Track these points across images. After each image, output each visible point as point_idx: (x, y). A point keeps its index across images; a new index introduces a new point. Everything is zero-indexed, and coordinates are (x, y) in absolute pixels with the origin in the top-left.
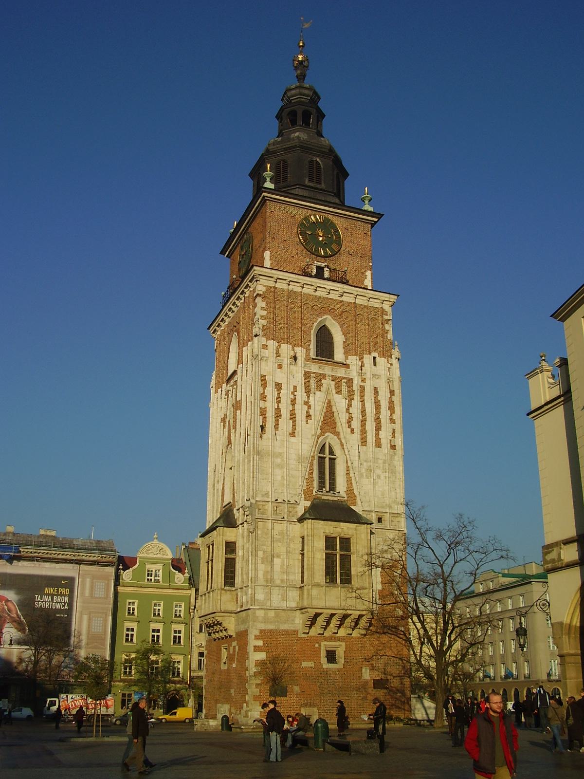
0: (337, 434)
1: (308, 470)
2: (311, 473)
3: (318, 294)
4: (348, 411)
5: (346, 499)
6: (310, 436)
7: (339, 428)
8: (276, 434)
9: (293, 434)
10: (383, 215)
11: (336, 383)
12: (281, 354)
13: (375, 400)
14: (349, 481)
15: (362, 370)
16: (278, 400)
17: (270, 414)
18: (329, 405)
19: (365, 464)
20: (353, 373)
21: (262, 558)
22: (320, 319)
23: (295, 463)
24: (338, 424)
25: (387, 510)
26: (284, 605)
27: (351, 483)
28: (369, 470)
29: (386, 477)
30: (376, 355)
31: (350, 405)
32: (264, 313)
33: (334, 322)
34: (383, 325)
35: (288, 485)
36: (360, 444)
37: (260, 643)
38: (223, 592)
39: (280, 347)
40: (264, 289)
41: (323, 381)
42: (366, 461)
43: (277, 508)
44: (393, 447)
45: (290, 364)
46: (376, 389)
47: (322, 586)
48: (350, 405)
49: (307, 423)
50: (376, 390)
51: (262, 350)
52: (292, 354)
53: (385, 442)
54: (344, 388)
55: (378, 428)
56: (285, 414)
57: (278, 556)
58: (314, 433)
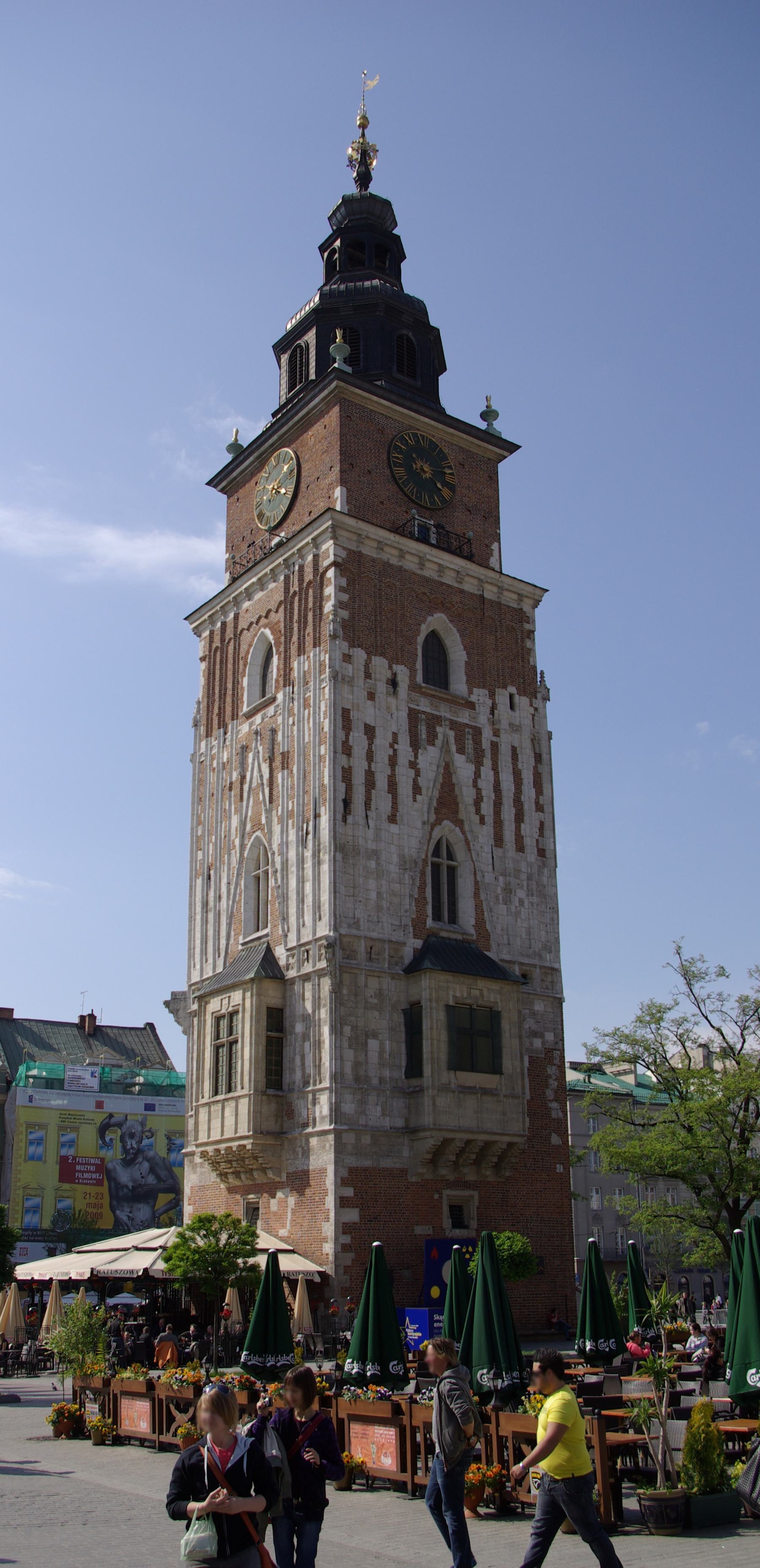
0: (460, 823)
1: (418, 883)
2: (422, 888)
3: (427, 573)
4: (475, 784)
5: (474, 938)
6: (419, 824)
7: (462, 815)
8: (367, 816)
9: (392, 819)
10: (519, 447)
11: (456, 736)
12: (373, 675)
13: (514, 769)
15: (492, 713)
16: (370, 756)
17: (359, 779)
18: (448, 771)
19: (501, 878)
20: (483, 719)
21: (349, 1038)
22: (430, 618)
23: (397, 870)
24: (461, 807)
25: (536, 961)
26: (387, 1122)
27: (482, 911)
28: (508, 890)
29: (532, 904)
30: (512, 689)
32: (345, 597)
33: (451, 625)
34: (523, 642)
35: (388, 909)
36: (492, 842)
37: (349, 1192)
38: (264, 1098)
39: (370, 659)
40: (344, 554)
41: (439, 729)
42: (502, 874)
43: (371, 948)
44: (542, 852)
45: (388, 694)
46: (514, 749)
47: (453, 1092)
49: (415, 800)
51: (344, 664)
52: (389, 675)
53: (529, 842)
54: (469, 744)
55: (519, 818)
56: (381, 782)
57: (375, 1036)
58: (426, 818)
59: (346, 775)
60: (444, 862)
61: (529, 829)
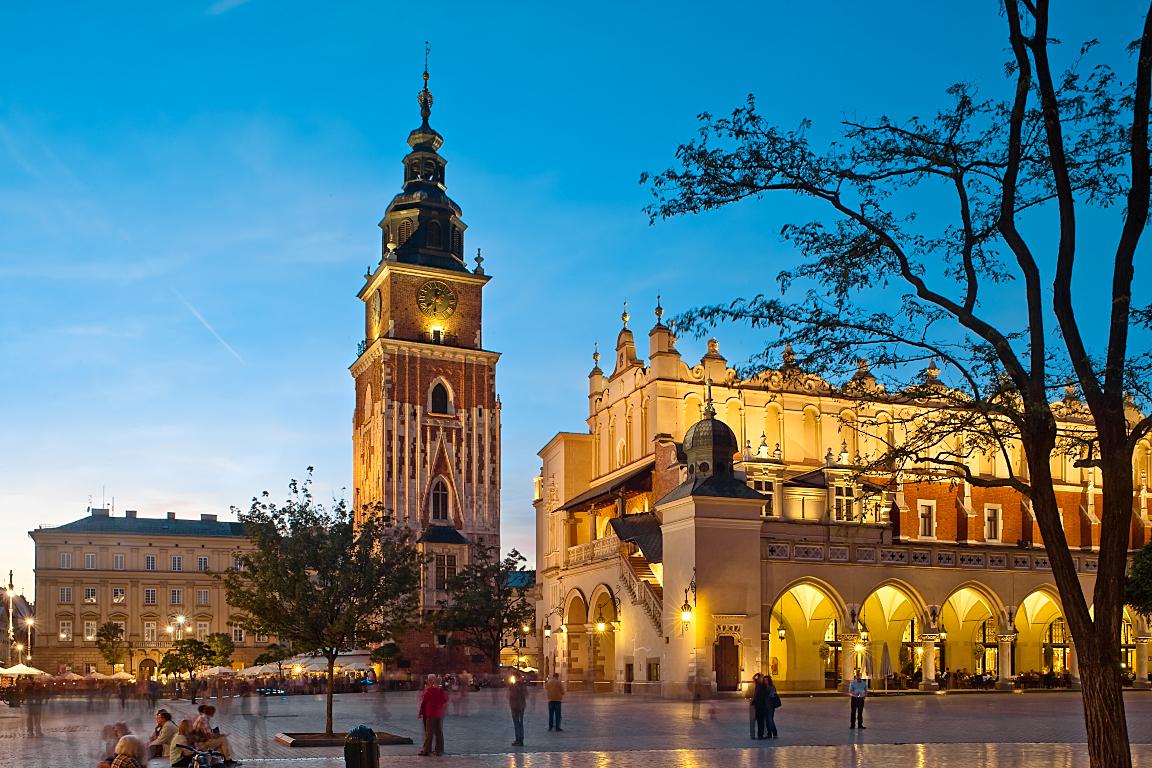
0: (448, 475)
4: (456, 454)
14: (456, 511)
16: (402, 450)
25: (488, 532)
31: (458, 451)
32: (389, 377)
48: (458, 451)
50: (480, 437)
52: (412, 411)
55: (481, 467)
59: (389, 461)
60: (440, 492)
61: (487, 473)
